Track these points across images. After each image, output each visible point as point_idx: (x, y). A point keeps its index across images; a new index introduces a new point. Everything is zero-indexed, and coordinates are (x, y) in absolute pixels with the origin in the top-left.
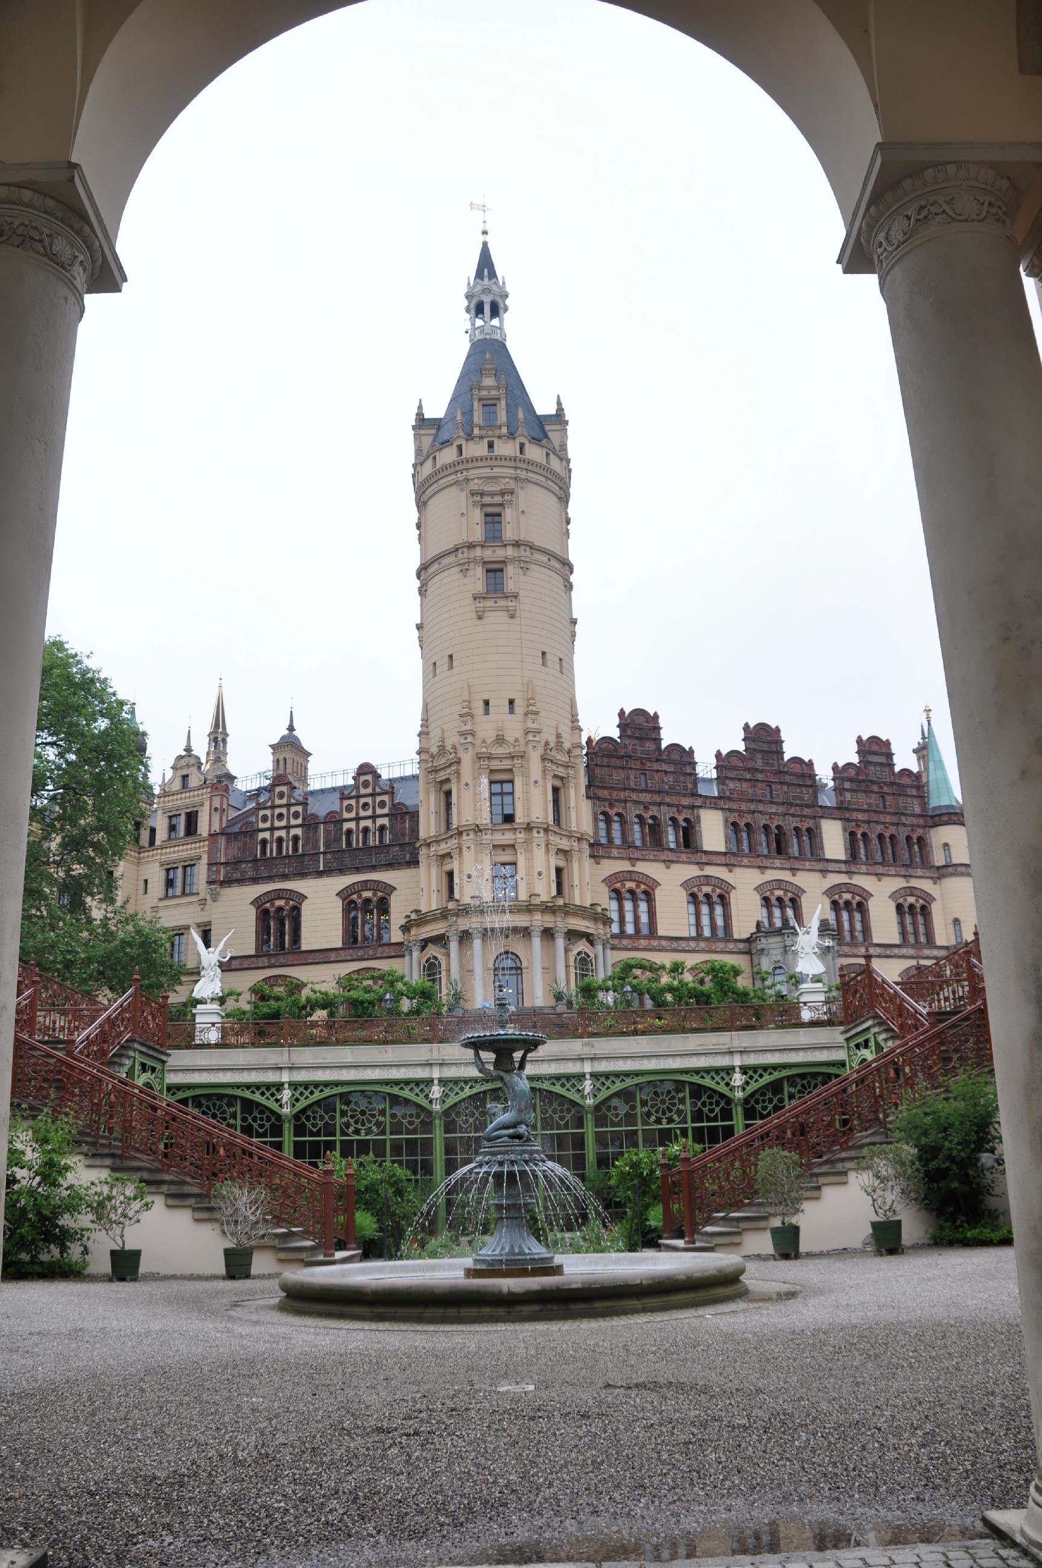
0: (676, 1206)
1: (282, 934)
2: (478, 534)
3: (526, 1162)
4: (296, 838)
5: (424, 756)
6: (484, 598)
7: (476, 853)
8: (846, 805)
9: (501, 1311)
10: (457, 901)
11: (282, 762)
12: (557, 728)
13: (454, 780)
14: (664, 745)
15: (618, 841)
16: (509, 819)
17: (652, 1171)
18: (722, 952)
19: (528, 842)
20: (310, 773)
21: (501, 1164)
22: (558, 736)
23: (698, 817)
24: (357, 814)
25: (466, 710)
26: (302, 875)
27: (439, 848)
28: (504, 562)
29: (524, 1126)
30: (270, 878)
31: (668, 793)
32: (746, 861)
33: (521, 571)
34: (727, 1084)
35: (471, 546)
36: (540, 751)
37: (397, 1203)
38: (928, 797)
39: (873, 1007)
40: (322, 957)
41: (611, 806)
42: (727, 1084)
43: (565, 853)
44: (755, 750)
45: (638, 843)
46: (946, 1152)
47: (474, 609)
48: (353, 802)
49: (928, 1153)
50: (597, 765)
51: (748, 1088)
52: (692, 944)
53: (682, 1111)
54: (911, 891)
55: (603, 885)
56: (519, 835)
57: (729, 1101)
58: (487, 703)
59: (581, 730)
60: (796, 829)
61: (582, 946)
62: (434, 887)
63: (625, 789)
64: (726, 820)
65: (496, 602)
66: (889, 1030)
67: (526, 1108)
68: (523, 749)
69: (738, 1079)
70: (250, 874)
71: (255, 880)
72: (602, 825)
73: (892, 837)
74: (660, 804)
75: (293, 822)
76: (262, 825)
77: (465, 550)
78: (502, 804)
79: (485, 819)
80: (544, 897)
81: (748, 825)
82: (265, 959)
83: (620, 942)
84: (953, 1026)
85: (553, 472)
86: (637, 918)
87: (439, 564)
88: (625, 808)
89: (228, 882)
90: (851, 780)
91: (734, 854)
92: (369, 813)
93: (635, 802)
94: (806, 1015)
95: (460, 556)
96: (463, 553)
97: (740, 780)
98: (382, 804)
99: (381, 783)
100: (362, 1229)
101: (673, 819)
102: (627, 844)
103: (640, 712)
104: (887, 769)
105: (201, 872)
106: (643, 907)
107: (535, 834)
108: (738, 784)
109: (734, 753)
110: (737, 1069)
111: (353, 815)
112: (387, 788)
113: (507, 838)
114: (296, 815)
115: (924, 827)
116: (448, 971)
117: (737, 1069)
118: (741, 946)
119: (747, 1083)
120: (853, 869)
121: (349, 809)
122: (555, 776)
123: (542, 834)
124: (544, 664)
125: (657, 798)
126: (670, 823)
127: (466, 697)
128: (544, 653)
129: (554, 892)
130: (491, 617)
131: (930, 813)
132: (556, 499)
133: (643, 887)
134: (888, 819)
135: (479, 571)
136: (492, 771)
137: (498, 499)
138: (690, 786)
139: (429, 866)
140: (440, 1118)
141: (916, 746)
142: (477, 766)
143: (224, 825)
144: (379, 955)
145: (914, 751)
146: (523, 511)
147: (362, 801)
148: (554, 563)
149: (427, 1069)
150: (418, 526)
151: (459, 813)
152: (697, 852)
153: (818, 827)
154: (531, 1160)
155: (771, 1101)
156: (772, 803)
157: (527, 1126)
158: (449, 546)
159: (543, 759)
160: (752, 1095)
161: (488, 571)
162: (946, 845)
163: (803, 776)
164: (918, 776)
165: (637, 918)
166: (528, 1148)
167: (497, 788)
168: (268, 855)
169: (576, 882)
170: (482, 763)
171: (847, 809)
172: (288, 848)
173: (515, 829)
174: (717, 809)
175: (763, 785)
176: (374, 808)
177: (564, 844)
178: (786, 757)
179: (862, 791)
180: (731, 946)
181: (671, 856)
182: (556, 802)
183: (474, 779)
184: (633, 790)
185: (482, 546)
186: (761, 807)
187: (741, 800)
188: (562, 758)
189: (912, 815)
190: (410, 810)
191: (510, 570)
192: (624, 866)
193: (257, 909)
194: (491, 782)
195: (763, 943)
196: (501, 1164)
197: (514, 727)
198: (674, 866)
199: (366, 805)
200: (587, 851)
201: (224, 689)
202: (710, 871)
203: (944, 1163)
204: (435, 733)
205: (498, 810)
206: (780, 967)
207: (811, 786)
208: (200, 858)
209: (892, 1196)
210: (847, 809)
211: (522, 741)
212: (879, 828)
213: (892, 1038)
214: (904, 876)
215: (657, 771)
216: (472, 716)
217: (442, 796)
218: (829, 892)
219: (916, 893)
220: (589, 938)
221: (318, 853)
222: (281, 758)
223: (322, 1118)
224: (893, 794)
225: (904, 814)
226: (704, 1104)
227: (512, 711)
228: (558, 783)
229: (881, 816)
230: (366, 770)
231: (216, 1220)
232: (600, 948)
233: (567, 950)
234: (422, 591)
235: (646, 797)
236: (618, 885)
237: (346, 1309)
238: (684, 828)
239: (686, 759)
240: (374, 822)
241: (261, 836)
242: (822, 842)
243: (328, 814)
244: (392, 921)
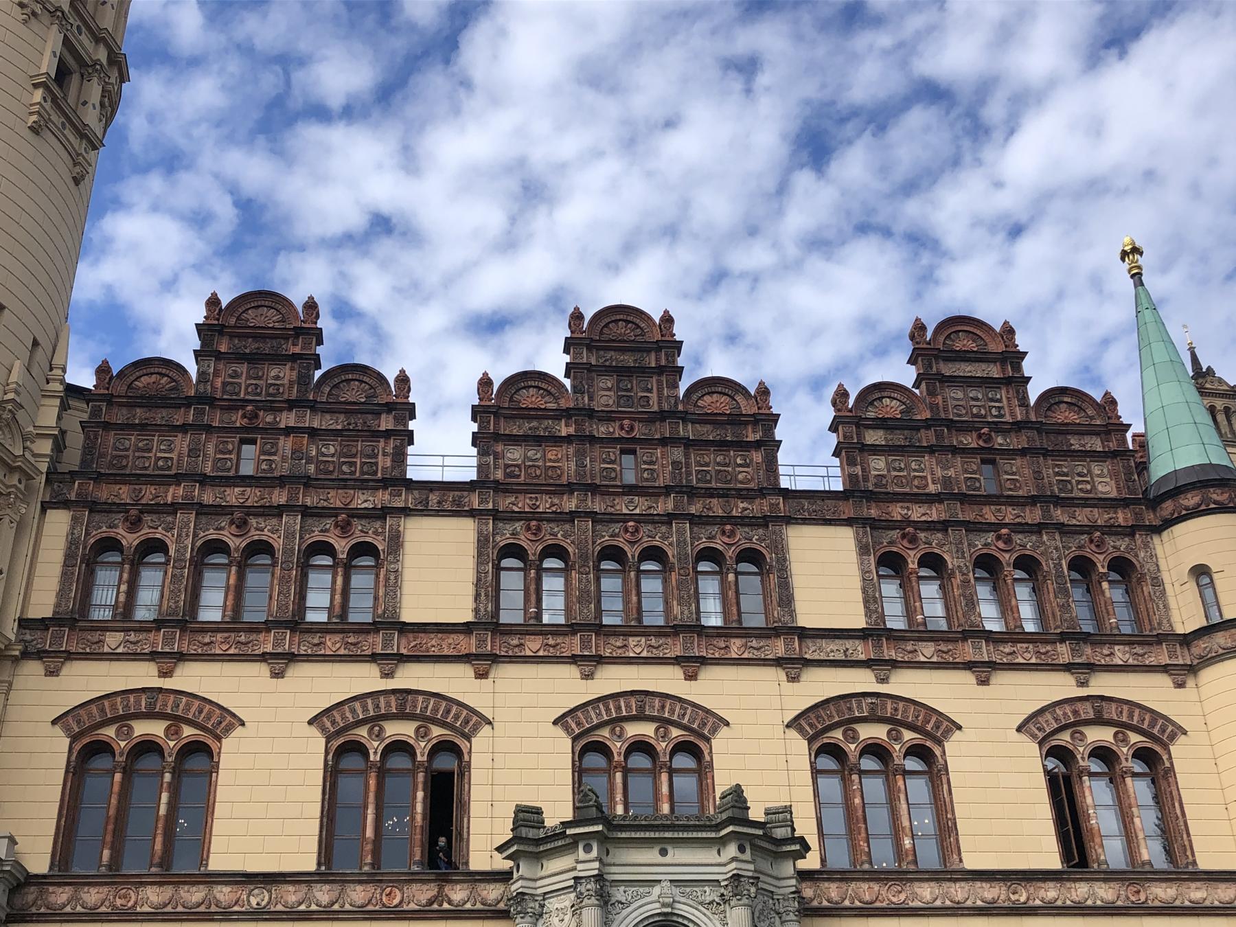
31: (308, 482)
44: (590, 368)
90: (882, 424)
104: (1003, 394)
115: (1130, 531)
120: (889, 653)
162: (1201, 572)
186: (597, 505)
202: (413, 677)
207: (758, 445)
210: (872, 497)
224: (1023, 452)
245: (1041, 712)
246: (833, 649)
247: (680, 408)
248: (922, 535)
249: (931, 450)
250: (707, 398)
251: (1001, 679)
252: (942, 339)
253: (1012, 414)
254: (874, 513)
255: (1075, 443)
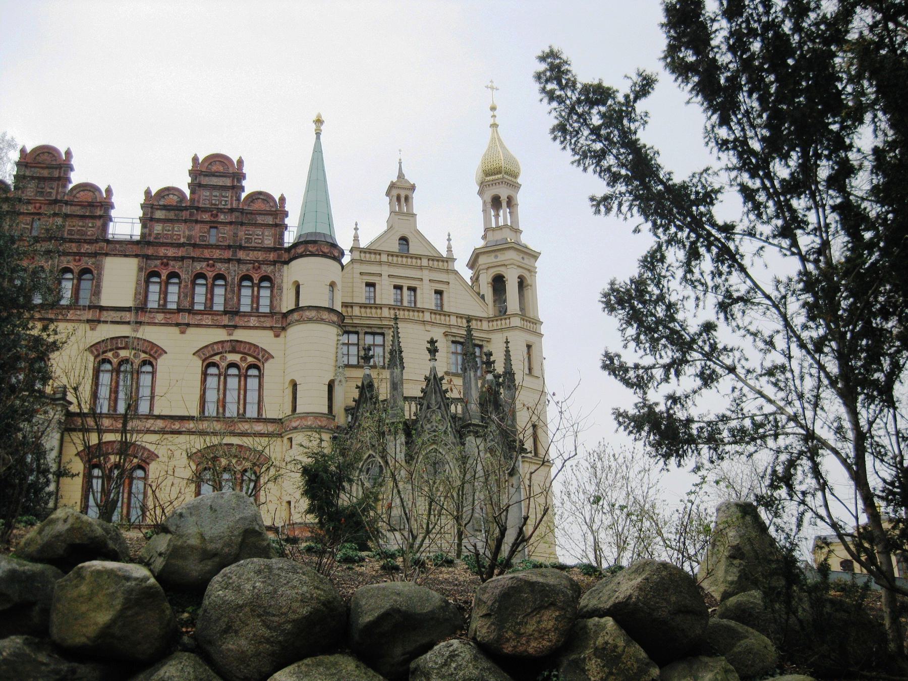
90: (165, 208)
104: (229, 194)
115: (274, 263)
153: (100, 268)
207: (100, 217)
210: (149, 243)
212: (199, 267)
224: (231, 223)
229: (206, 251)
245: (206, 347)
246: (116, 316)
247: (66, 198)
248: (172, 263)
249: (185, 221)
250: (82, 193)
251: (191, 331)
252: (206, 164)
253: (232, 204)
254: (150, 251)
255: (260, 219)
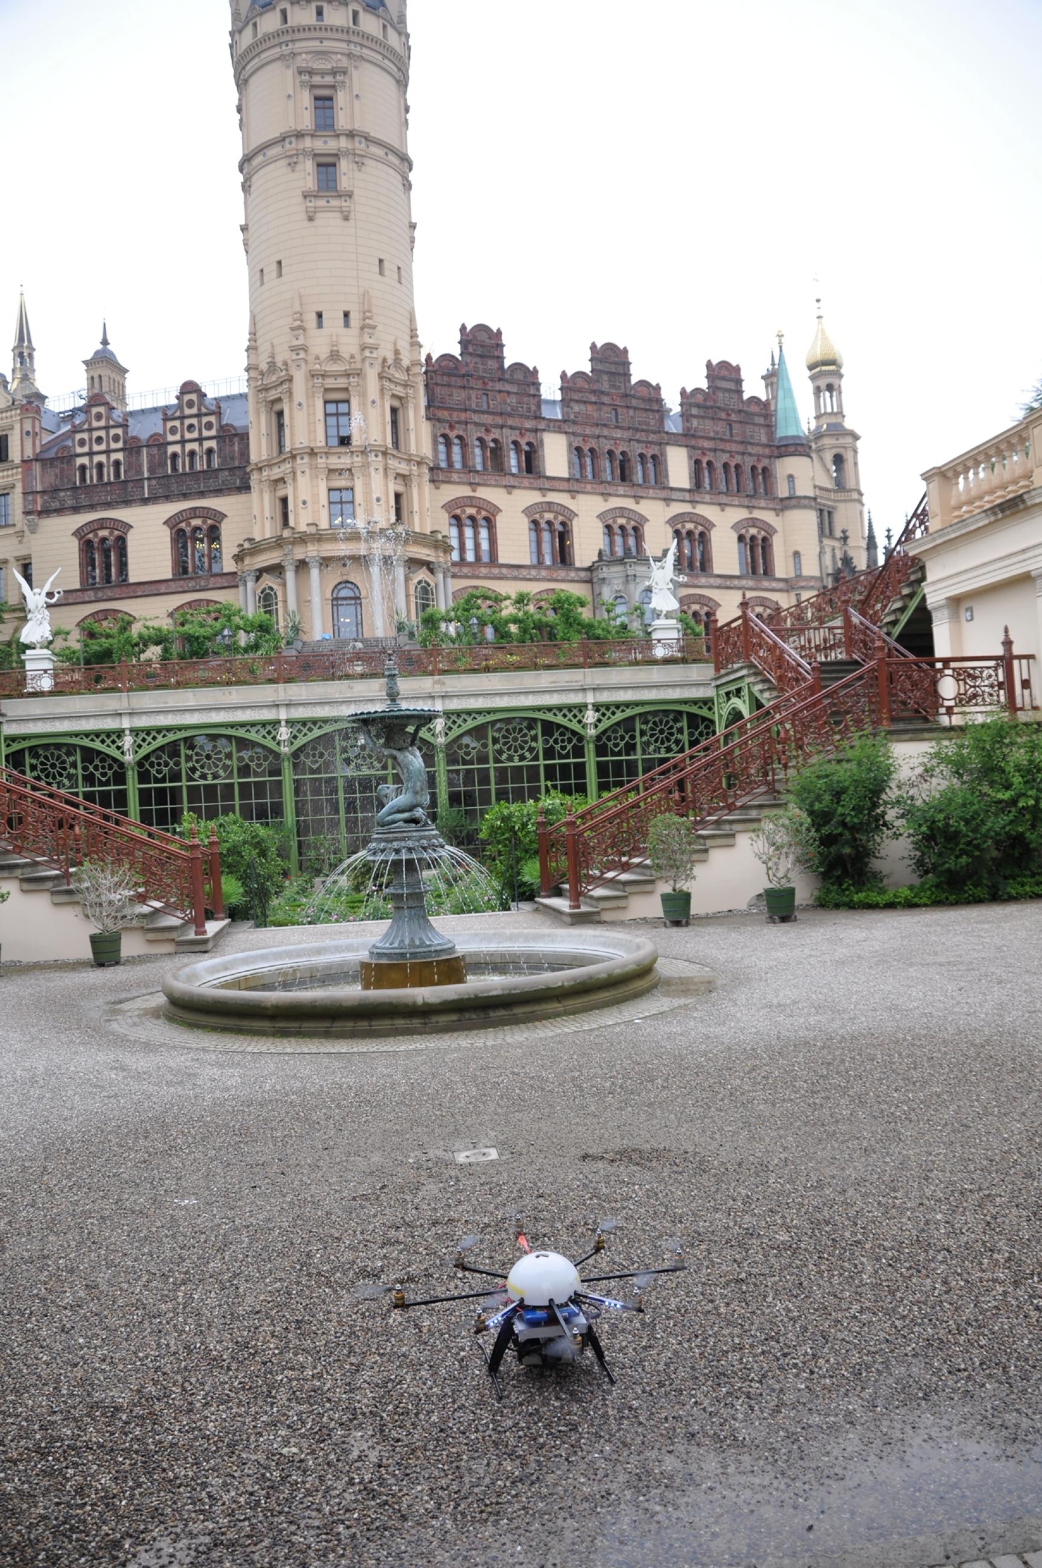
0: (554, 864)
1: (108, 567)
2: (307, 121)
3: (425, 849)
4: (117, 463)
5: (253, 374)
6: (315, 196)
7: (312, 478)
8: (692, 432)
9: (416, 1022)
10: (293, 528)
11: (96, 380)
12: (395, 344)
13: (286, 400)
14: (507, 364)
15: (458, 465)
16: (345, 441)
17: (524, 825)
18: (563, 581)
19: (366, 466)
20: (128, 391)
21: (397, 851)
22: (397, 352)
23: (542, 441)
24: (182, 436)
25: (298, 323)
26: (127, 503)
27: (271, 473)
28: (336, 155)
29: (420, 809)
30: (92, 507)
31: (510, 415)
32: (589, 487)
33: (355, 166)
34: (580, 722)
35: (299, 135)
36: (378, 368)
37: (261, 864)
38: (775, 426)
39: (748, 657)
40: (152, 589)
41: (451, 427)
42: (580, 722)
43: (404, 478)
44: (601, 371)
45: (479, 467)
46: (840, 818)
47: (304, 209)
48: (177, 423)
49: (820, 818)
50: (437, 384)
51: (600, 725)
52: (534, 572)
53: (534, 748)
54: (754, 522)
55: (443, 511)
56: (356, 459)
57: (581, 738)
58: (320, 315)
59: (421, 346)
60: (641, 456)
61: (422, 575)
62: (267, 514)
63: (466, 410)
64: (570, 445)
65: (328, 202)
66: (766, 681)
67: (422, 790)
68: (359, 366)
69: (590, 716)
70: (70, 503)
71: (76, 509)
72: (442, 448)
73: (737, 467)
74: (502, 427)
75: (114, 446)
76: (79, 450)
77: (293, 139)
78: (338, 426)
79: (320, 441)
80: (383, 524)
81: (592, 450)
82: (91, 593)
83: (460, 571)
84: (846, 686)
85: (392, 51)
86: (477, 546)
87: (264, 155)
88: (466, 430)
89: (46, 512)
90: (698, 406)
91: (577, 480)
92: (195, 435)
93: (476, 424)
94: (659, 652)
95: (287, 146)
96: (291, 143)
97: (585, 402)
98: (209, 426)
99: (207, 403)
100: (229, 897)
101: (515, 443)
102: (468, 468)
103: (481, 328)
104: (735, 396)
105: (17, 500)
106: (484, 533)
107: (374, 458)
108: (582, 407)
109: (579, 374)
110: (590, 707)
111: (178, 437)
112: (213, 408)
113: (344, 461)
114: (116, 438)
115: (770, 457)
116: (285, 601)
117: (590, 707)
118: (583, 574)
119: (599, 721)
120: (697, 499)
121: (173, 431)
122: (394, 396)
123: (380, 458)
124: (381, 273)
125: (499, 420)
126: (512, 446)
127: (297, 308)
128: (381, 261)
129: (393, 519)
130: (322, 219)
131: (776, 443)
132: (393, 82)
133: (484, 513)
134: (734, 447)
135: (309, 165)
136: (326, 390)
137: (328, 80)
138: (533, 408)
139: (261, 491)
140: (289, 759)
141: (764, 373)
142: (310, 384)
143: (38, 450)
144: (211, 586)
145: (763, 378)
146: (357, 96)
147: (187, 422)
148: (392, 158)
149: (274, 710)
150: (239, 110)
151: (292, 435)
152: (540, 477)
153: (663, 454)
154: (429, 846)
155: (622, 738)
156: (617, 427)
157: (423, 808)
158: (274, 133)
159: (381, 377)
160: (604, 732)
161: (319, 165)
163: (650, 400)
164: (766, 405)
165: (477, 546)
166: (426, 833)
167: (332, 408)
168: (88, 481)
169: (416, 508)
170: (316, 381)
171: (693, 436)
172: (109, 475)
173: (352, 452)
174: (560, 432)
175: (609, 409)
176: (200, 430)
177: (403, 468)
178: (634, 380)
179: (708, 418)
180: (573, 574)
181: (512, 481)
182: (394, 423)
183: (308, 398)
184: (475, 411)
185: (312, 136)
186: (605, 432)
187: (586, 424)
188: (400, 376)
189: (758, 444)
190: (239, 432)
191: (344, 165)
192: (464, 491)
193: (80, 540)
194: (326, 402)
195: (605, 572)
196: (397, 851)
197: (349, 343)
198: (516, 492)
199: (191, 427)
200: (427, 476)
201: (26, 297)
202: (553, 497)
203: (836, 828)
204: (264, 349)
205: (333, 432)
206: (621, 597)
207: (658, 411)
208: (13, 487)
209: (786, 864)
210: (693, 436)
211: (358, 358)
213: (769, 689)
214: (748, 507)
215: (500, 391)
216: (304, 330)
217: (274, 417)
218: (672, 521)
219: (758, 524)
220: (429, 566)
221: (142, 480)
222: (96, 376)
223: (166, 764)
225: (751, 444)
226: (556, 741)
227: (347, 324)
228: (396, 404)
229: (728, 444)
230: (189, 388)
231: (78, 903)
232: (441, 576)
233: (407, 579)
234: (246, 187)
235: (488, 419)
236: (458, 511)
237: (246, 1024)
238: (526, 452)
239: (530, 380)
240: (201, 445)
241: (80, 461)
242: (666, 470)
243: (151, 437)
244: (224, 551)
254: (693, 442)
